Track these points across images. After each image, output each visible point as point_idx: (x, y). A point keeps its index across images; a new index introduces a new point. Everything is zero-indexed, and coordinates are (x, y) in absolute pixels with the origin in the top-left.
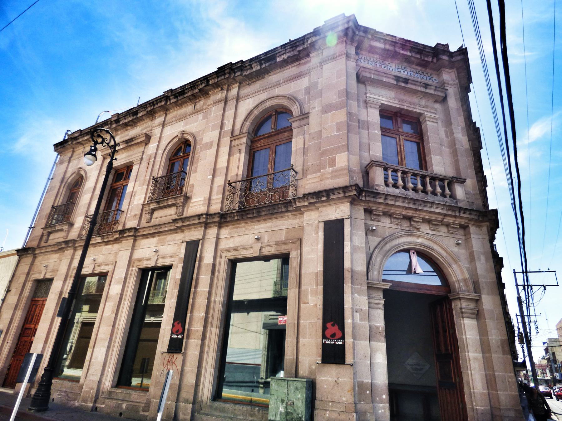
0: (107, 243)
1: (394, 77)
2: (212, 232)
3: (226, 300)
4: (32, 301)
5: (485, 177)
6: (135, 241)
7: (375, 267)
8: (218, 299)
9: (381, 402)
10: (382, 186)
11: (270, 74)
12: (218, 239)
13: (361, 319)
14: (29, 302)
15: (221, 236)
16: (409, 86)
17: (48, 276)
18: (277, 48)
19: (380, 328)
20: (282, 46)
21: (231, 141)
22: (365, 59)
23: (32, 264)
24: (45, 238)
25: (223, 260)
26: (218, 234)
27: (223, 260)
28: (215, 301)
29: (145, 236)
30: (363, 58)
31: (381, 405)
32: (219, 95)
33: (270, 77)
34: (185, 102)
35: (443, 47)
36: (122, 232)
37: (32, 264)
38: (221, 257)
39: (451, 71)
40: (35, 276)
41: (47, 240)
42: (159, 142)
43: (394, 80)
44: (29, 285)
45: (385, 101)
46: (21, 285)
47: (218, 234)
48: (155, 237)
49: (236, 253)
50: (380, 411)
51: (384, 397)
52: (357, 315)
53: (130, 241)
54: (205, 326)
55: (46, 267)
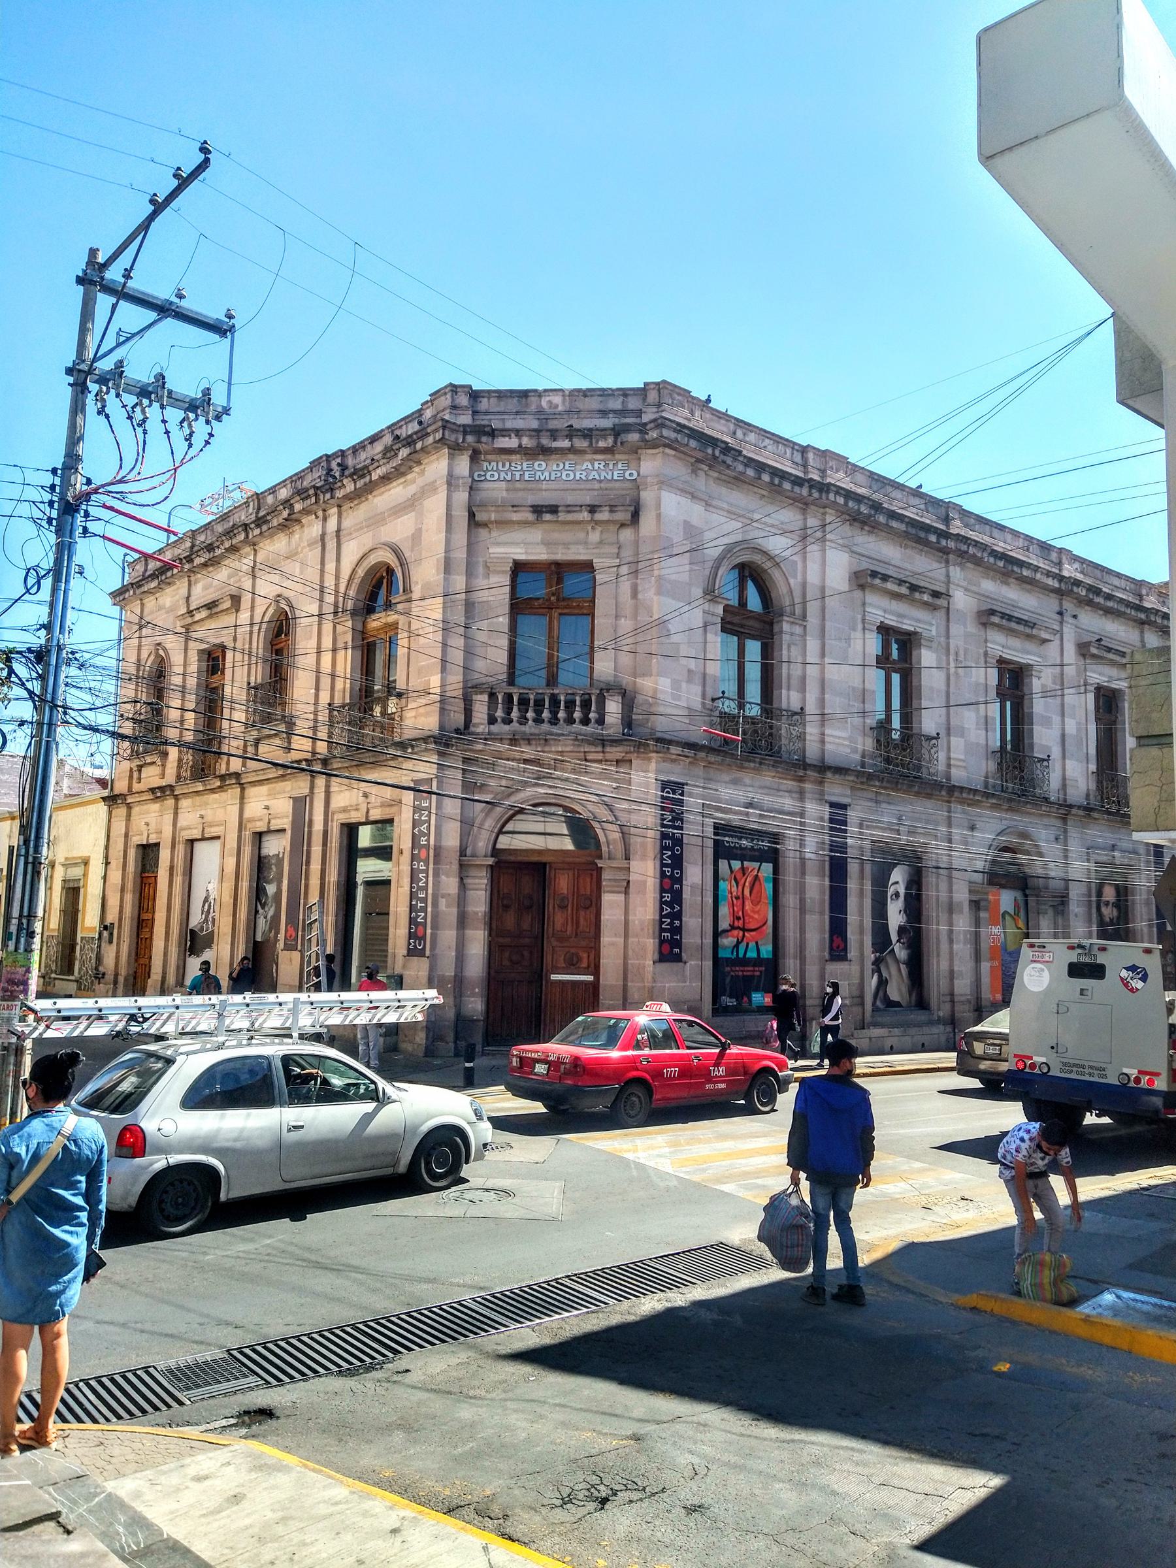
0: (212, 791)
2: (321, 781)
3: (343, 879)
4: (142, 878)
5: (958, 535)
6: (243, 790)
9: (473, 995)
12: (328, 794)
13: (447, 906)
14: (139, 880)
15: (332, 789)
16: (562, 516)
17: (153, 839)
20: (388, 427)
23: (129, 816)
24: (136, 775)
26: (328, 787)
29: (253, 783)
32: (312, 528)
33: (376, 500)
34: (272, 536)
36: (222, 778)
37: (129, 816)
39: (657, 451)
40: (138, 839)
41: (139, 779)
42: (253, 608)
44: (132, 853)
46: (122, 853)
47: (328, 787)
52: (443, 903)
53: (237, 790)
55: (147, 824)
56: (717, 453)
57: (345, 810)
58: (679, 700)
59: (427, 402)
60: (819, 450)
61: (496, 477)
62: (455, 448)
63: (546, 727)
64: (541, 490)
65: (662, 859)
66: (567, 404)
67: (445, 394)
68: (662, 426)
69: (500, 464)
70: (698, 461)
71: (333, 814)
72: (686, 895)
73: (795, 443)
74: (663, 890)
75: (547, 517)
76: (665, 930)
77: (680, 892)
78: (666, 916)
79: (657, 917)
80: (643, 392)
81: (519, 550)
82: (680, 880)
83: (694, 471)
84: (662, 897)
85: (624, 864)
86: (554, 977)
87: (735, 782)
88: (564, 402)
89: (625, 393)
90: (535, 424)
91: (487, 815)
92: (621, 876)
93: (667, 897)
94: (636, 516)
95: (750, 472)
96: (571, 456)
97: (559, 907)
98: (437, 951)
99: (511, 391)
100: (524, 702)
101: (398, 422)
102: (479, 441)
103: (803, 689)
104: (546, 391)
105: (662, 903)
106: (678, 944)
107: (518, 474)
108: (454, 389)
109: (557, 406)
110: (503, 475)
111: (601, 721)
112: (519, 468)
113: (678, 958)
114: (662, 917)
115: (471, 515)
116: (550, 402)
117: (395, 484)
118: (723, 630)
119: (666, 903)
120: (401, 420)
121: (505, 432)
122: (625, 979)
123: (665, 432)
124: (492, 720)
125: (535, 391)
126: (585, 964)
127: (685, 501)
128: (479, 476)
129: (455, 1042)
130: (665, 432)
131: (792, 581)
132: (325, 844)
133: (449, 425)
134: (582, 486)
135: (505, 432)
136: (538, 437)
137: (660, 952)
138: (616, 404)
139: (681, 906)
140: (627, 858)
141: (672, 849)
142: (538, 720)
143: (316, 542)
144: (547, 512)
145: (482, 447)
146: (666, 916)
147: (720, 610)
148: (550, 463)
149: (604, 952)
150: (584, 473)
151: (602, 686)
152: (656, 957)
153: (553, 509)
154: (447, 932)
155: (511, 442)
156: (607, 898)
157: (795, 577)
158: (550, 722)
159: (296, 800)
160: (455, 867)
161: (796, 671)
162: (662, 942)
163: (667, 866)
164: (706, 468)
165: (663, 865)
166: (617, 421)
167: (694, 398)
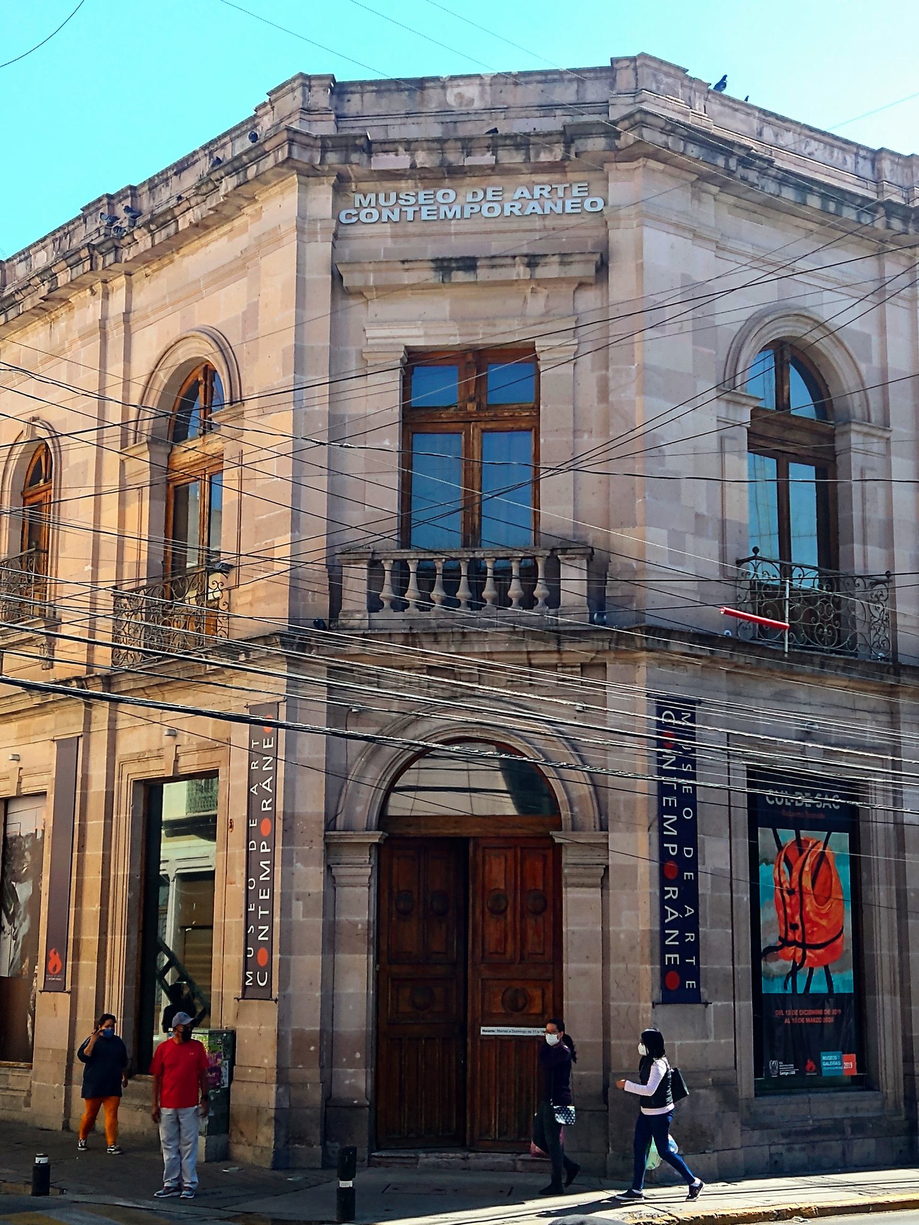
1: (432, 265)
2: (101, 712)
3: (138, 871)
7: (361, 796)
8: (120, 873)
9: (352, 1064)
10: (358, 612)
11: (182, 252)
12: (113, 732)
13: (306, 913)
15: (120, 725)
16: (483, 274)
18: (195, 153)
19: (360, 926)
20: (204, 148)
21: (122, 462)
22: (373, 204)
25: (124, 781)
26: (113, 721)
27: (124, 781)
28: (116, 876)
30: (365, 204)
31: (351, 1071)
33: (187, 261)
34: (23, 326)
35: (632, 65)
38: (120, 777)
39: (634, 164)
43: (436, 269)
45: (418, 337)
47: (113, 721)
48: (11, 721)
49: (143, 767)
50: (347, 1082)
51: (358, 1055)
52: (298, 907)
54: (103, 932)
56: (733, 163)
57: (140, 758)
58: (681, 565)
59: (265, 104)
60: (899, 156)
61: (375, 218)
62: (310, 173)
63: (463, 611)
64: (450, 234)
65: (662, 829)
66: (488, 98)
67: (293, 90)
68: (642, 124)
69: (382, 196)
70: (704, 178)
71: (121, 765)
72: (705, 888)
73: (859, 146)
74: (664, 881)
75: (459, 276)
76: (671, 949)
77: (694, 883)
78: (671, 925)
79: (657, 928)
80: (609, 73)
81: (415, 332)
82: (692, 865)
83: (696, 196)
84: (663, 893)
85: (596, 837)
86: (486, 1031)
87: (780, 697)
88: (482, 94)
89: (580, 76)
90: (436, 131)
91: (368, 761)
92: (594, 858)
93: (673, 892)
94: (603, 268)
95: (789, 194)
96: (496, 179)
97: (492, 911)
98: (290, 990)
99: (397, 82)
100: (426, 574)
101: (220, 138)
102: (347, 161)
103: (888, 542)
104: (453, 78)
105: (663, 902)
106: (694, 972)
107: (410, 211)
108: (306, 81)
109: (472, 101)
110: (386, 213)
111: (553, 600)
112: (412, 200)
113: (694, 997)
114: (664, 926)
115: (337, 278)
116: (460, 96)
117: (215, 234)
118: (752, 448)
119: (670, 902)
120: (224, 135)
121: (389, 146)
122: (606, 1033)
123: (648, 134)
124: (374, 605)
125: (437, 79)
126: (537, 1009)
127: (683, 243)
128: (349, 216)
129: (323, 1144)
130: (647, 134)
131: (863, 367)
132: (108, 815)
133: (298, 137)
134: (515, 226)
135: (389, 146)
136: (443, 151)
137: (664, 987)
138: (566, 94)
139: (696, 907)
140: (604, 828)
141: (677, 811)
142: (451, 602)
143: (92, 333)
144: (458, 269)
145: (352, 171)
146: (671, 925)
147: (745, 416)
148: (462, 191)
149: (570, 986)
150: (518, 205)
151: (555, 543)
152: (658, 994)
153: (469, 264)
154: (308, 958)
155: (400, 161)
156: (570, 895)
157: (869, 360)
158: (469, 605)
159: (62, 744)
160: (318, 847)
161: (877, 514)
162: (666, 970)
163: (671, 839)
164: (715, 189)
165: (663, 839)
166: (568, 119)
167: (692, 80)
